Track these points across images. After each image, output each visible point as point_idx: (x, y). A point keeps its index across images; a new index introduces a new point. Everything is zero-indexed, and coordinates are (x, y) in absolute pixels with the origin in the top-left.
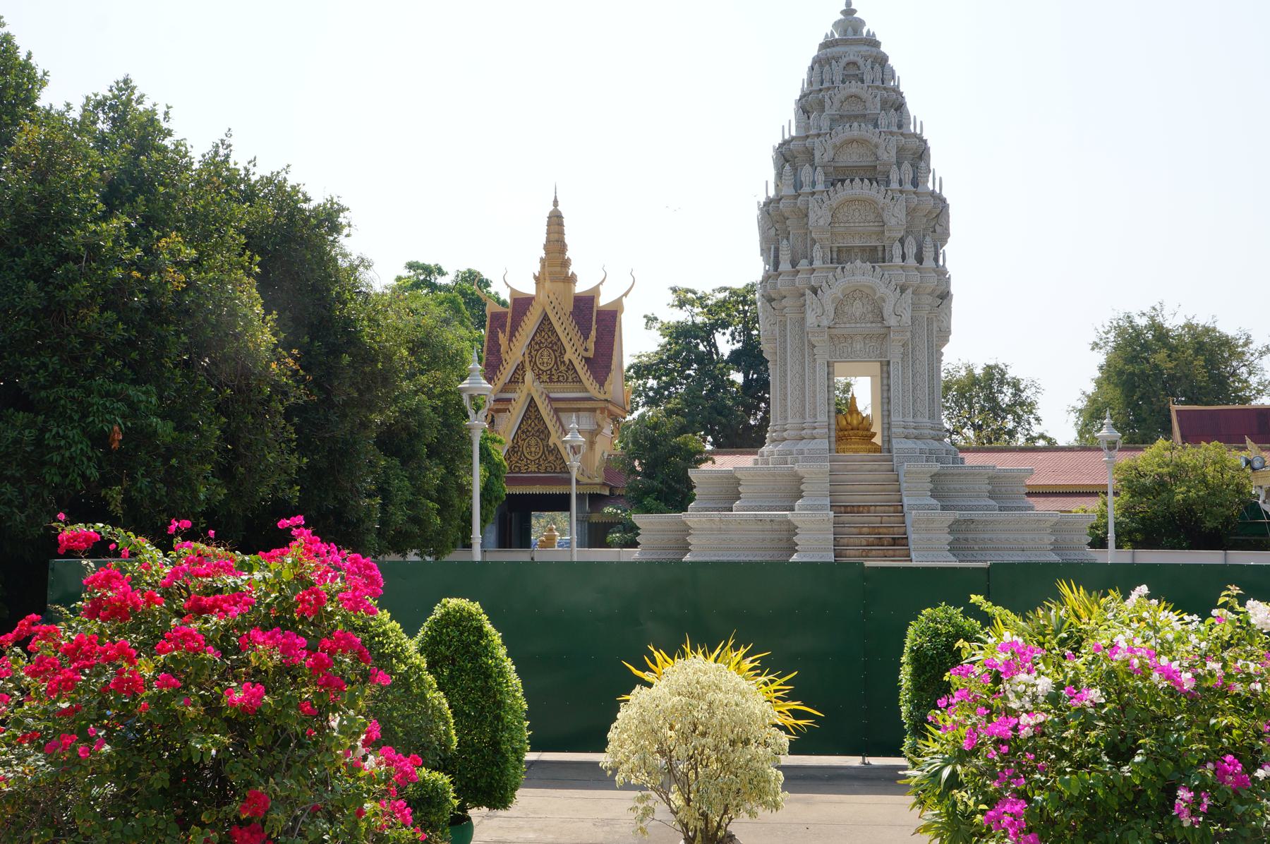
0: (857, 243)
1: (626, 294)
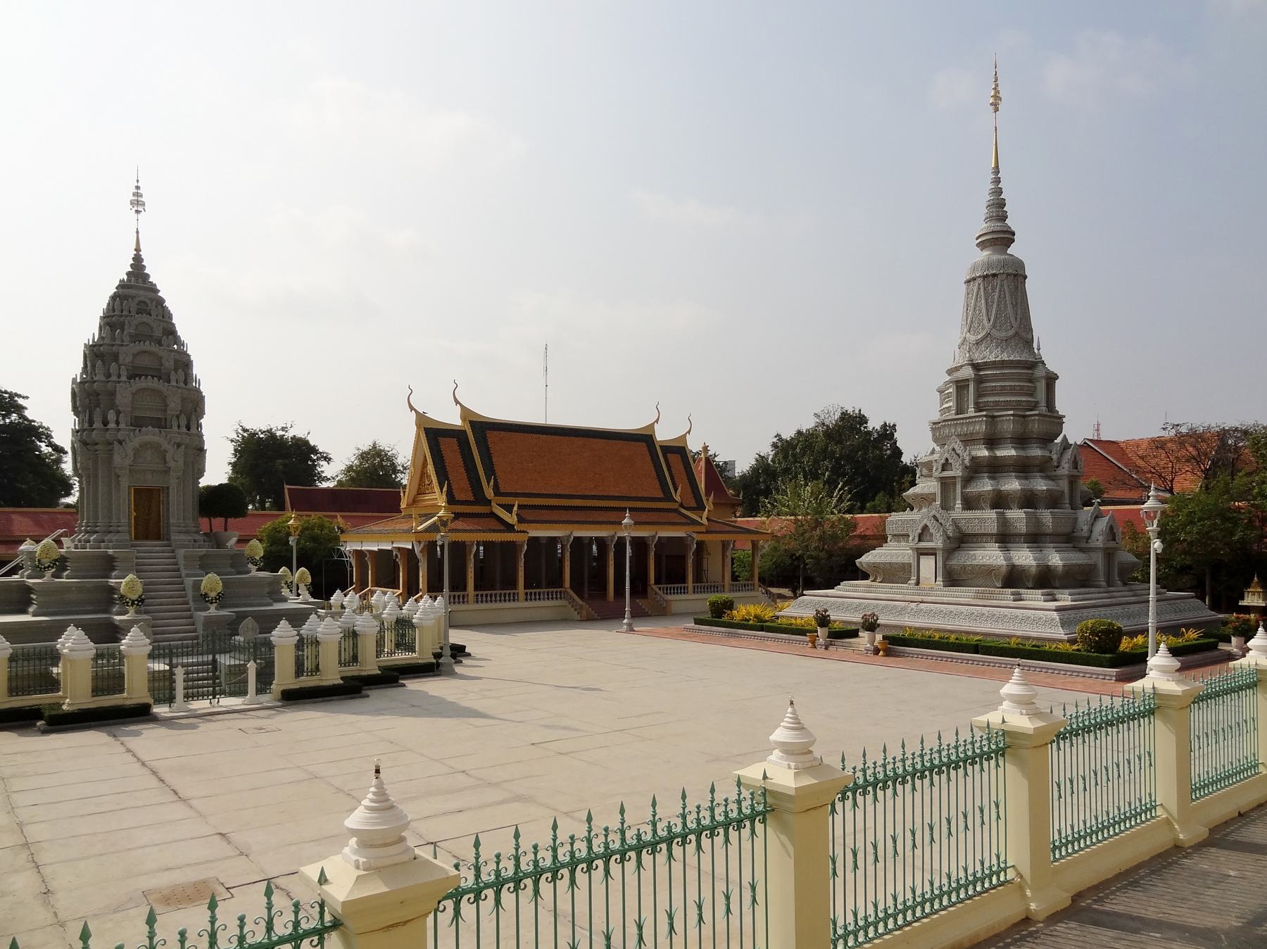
0: (148, 414)
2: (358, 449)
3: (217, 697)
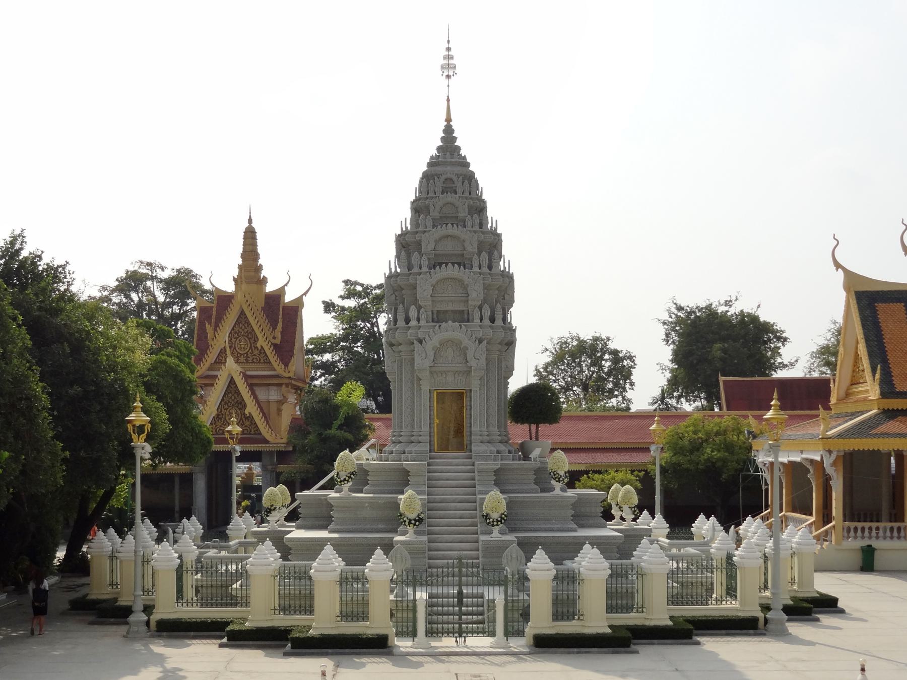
0: (450, 307)
1: (305, 294)
2: (835, 323)
3: (464, 635)
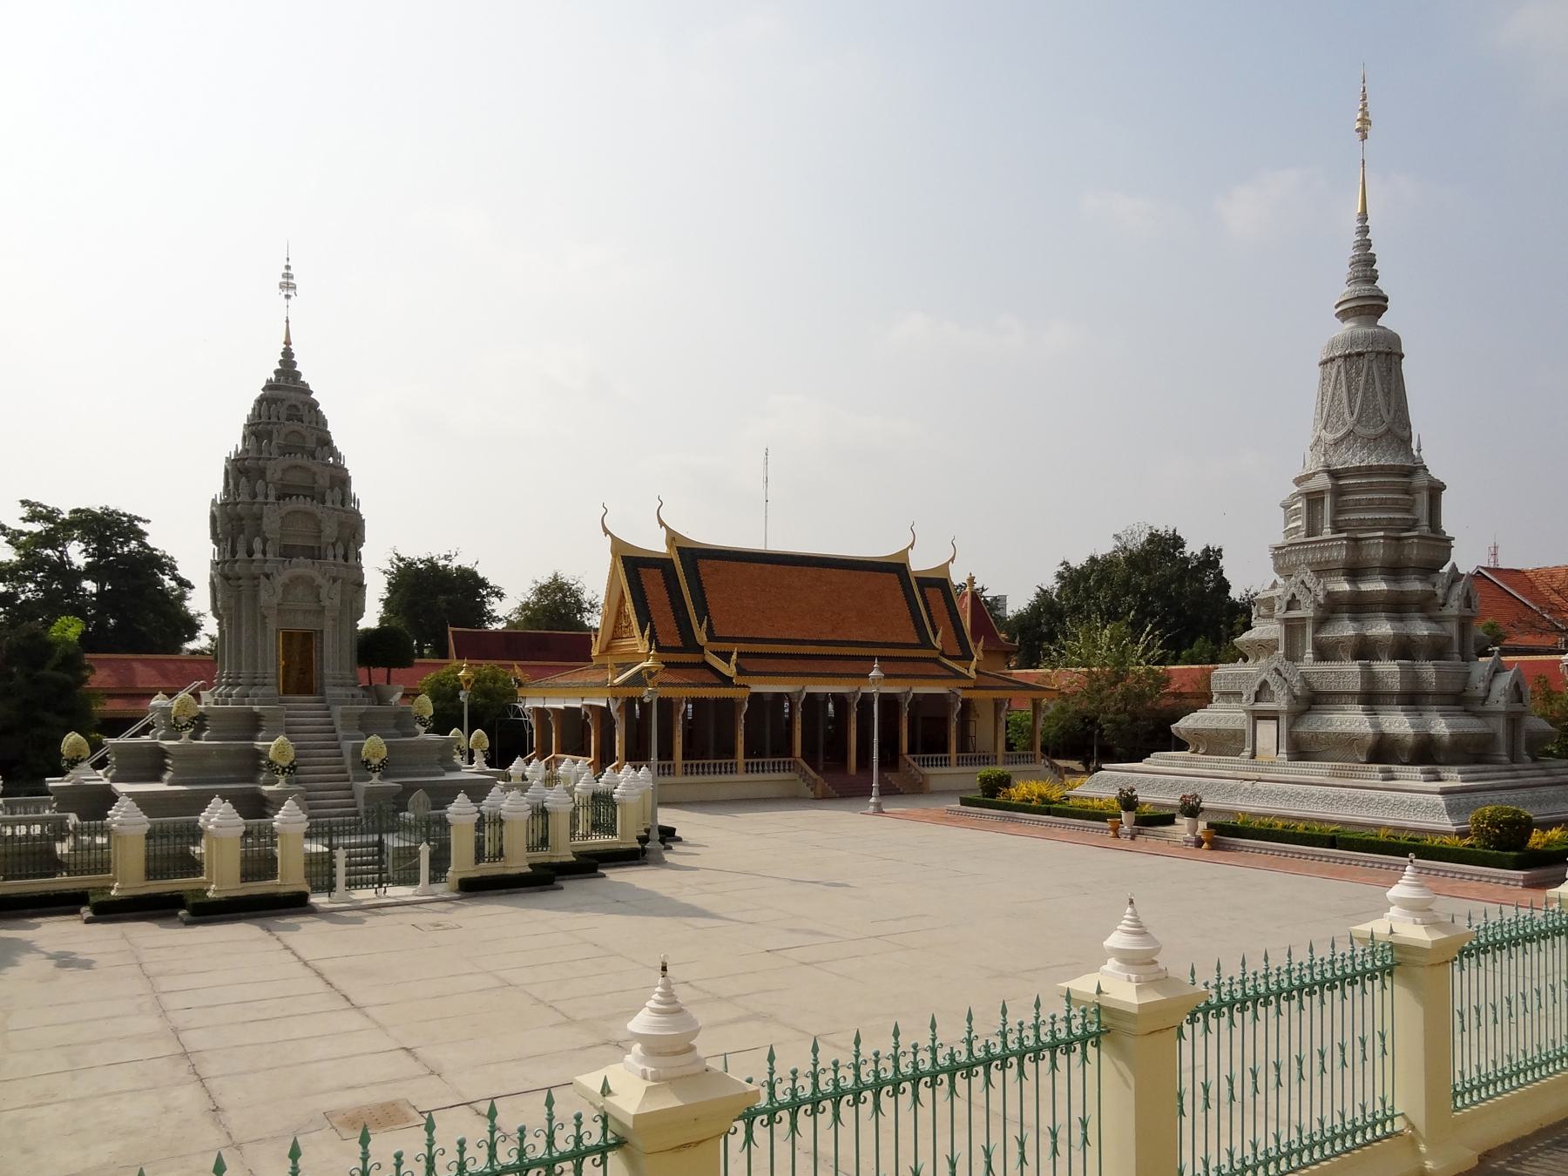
0: (299, 542)
2: (536, 582)
3: (385, 885)
